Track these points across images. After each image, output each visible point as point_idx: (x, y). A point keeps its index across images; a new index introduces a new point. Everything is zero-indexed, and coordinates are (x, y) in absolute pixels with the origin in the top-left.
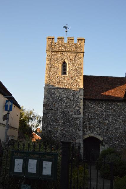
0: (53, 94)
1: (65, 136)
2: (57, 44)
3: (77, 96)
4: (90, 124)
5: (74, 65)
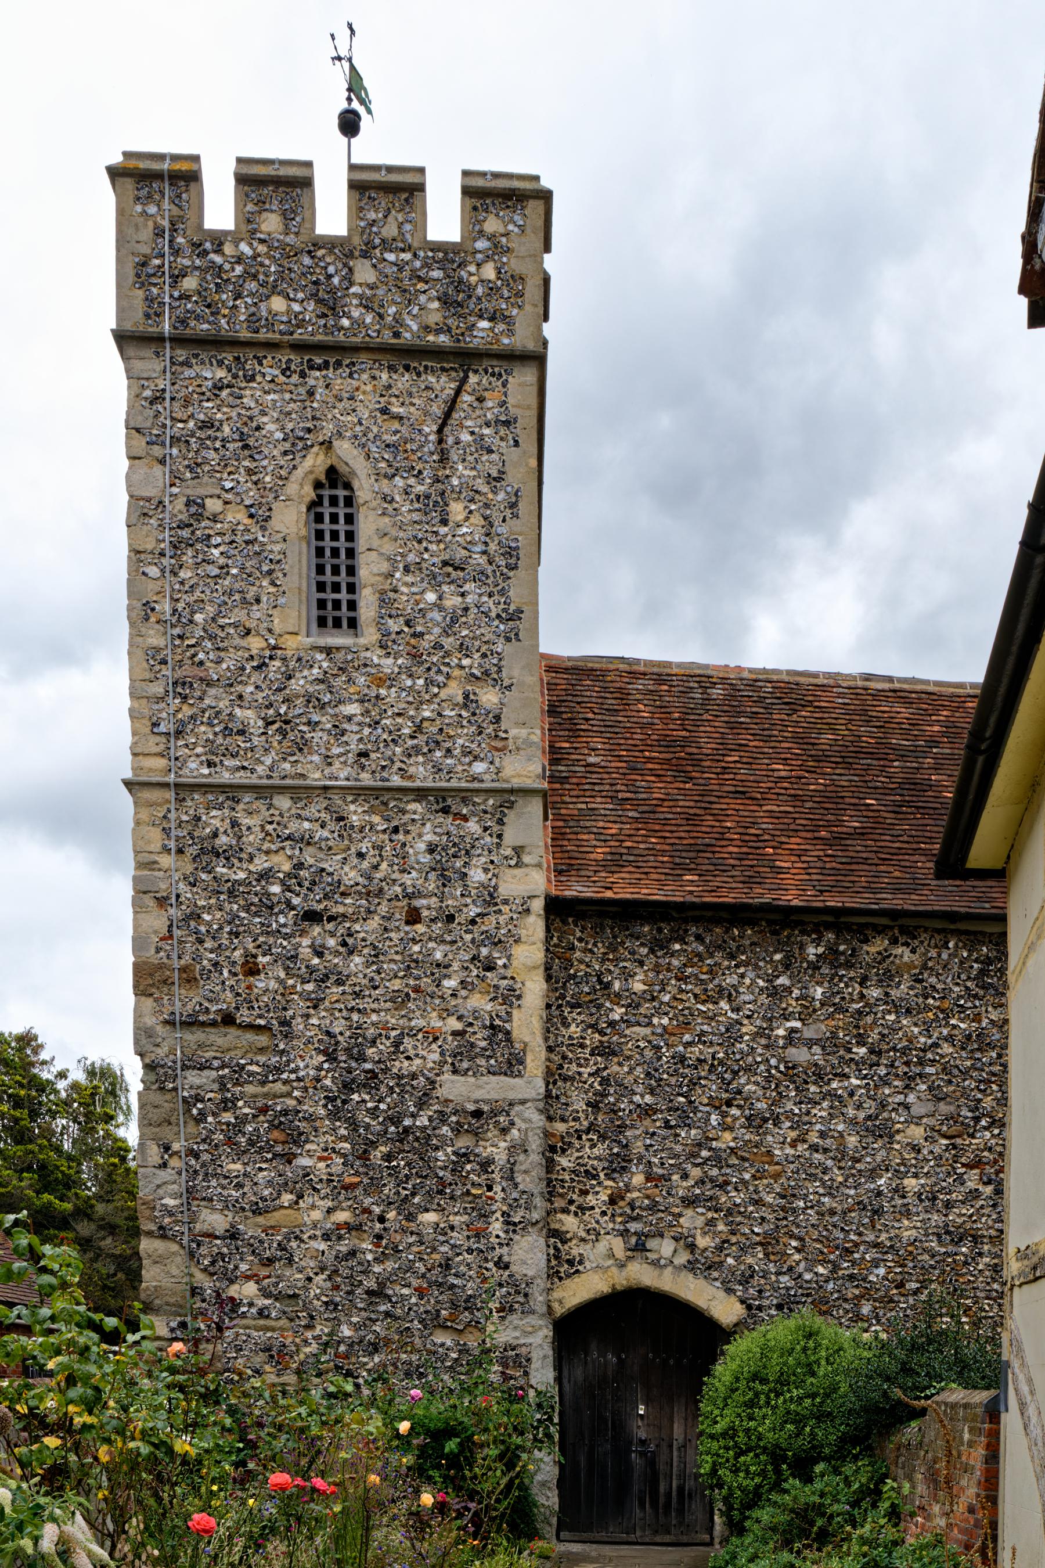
0: (227, 856)
1: (370, 1293)
4: (619, 1165)
5: (434, 506)
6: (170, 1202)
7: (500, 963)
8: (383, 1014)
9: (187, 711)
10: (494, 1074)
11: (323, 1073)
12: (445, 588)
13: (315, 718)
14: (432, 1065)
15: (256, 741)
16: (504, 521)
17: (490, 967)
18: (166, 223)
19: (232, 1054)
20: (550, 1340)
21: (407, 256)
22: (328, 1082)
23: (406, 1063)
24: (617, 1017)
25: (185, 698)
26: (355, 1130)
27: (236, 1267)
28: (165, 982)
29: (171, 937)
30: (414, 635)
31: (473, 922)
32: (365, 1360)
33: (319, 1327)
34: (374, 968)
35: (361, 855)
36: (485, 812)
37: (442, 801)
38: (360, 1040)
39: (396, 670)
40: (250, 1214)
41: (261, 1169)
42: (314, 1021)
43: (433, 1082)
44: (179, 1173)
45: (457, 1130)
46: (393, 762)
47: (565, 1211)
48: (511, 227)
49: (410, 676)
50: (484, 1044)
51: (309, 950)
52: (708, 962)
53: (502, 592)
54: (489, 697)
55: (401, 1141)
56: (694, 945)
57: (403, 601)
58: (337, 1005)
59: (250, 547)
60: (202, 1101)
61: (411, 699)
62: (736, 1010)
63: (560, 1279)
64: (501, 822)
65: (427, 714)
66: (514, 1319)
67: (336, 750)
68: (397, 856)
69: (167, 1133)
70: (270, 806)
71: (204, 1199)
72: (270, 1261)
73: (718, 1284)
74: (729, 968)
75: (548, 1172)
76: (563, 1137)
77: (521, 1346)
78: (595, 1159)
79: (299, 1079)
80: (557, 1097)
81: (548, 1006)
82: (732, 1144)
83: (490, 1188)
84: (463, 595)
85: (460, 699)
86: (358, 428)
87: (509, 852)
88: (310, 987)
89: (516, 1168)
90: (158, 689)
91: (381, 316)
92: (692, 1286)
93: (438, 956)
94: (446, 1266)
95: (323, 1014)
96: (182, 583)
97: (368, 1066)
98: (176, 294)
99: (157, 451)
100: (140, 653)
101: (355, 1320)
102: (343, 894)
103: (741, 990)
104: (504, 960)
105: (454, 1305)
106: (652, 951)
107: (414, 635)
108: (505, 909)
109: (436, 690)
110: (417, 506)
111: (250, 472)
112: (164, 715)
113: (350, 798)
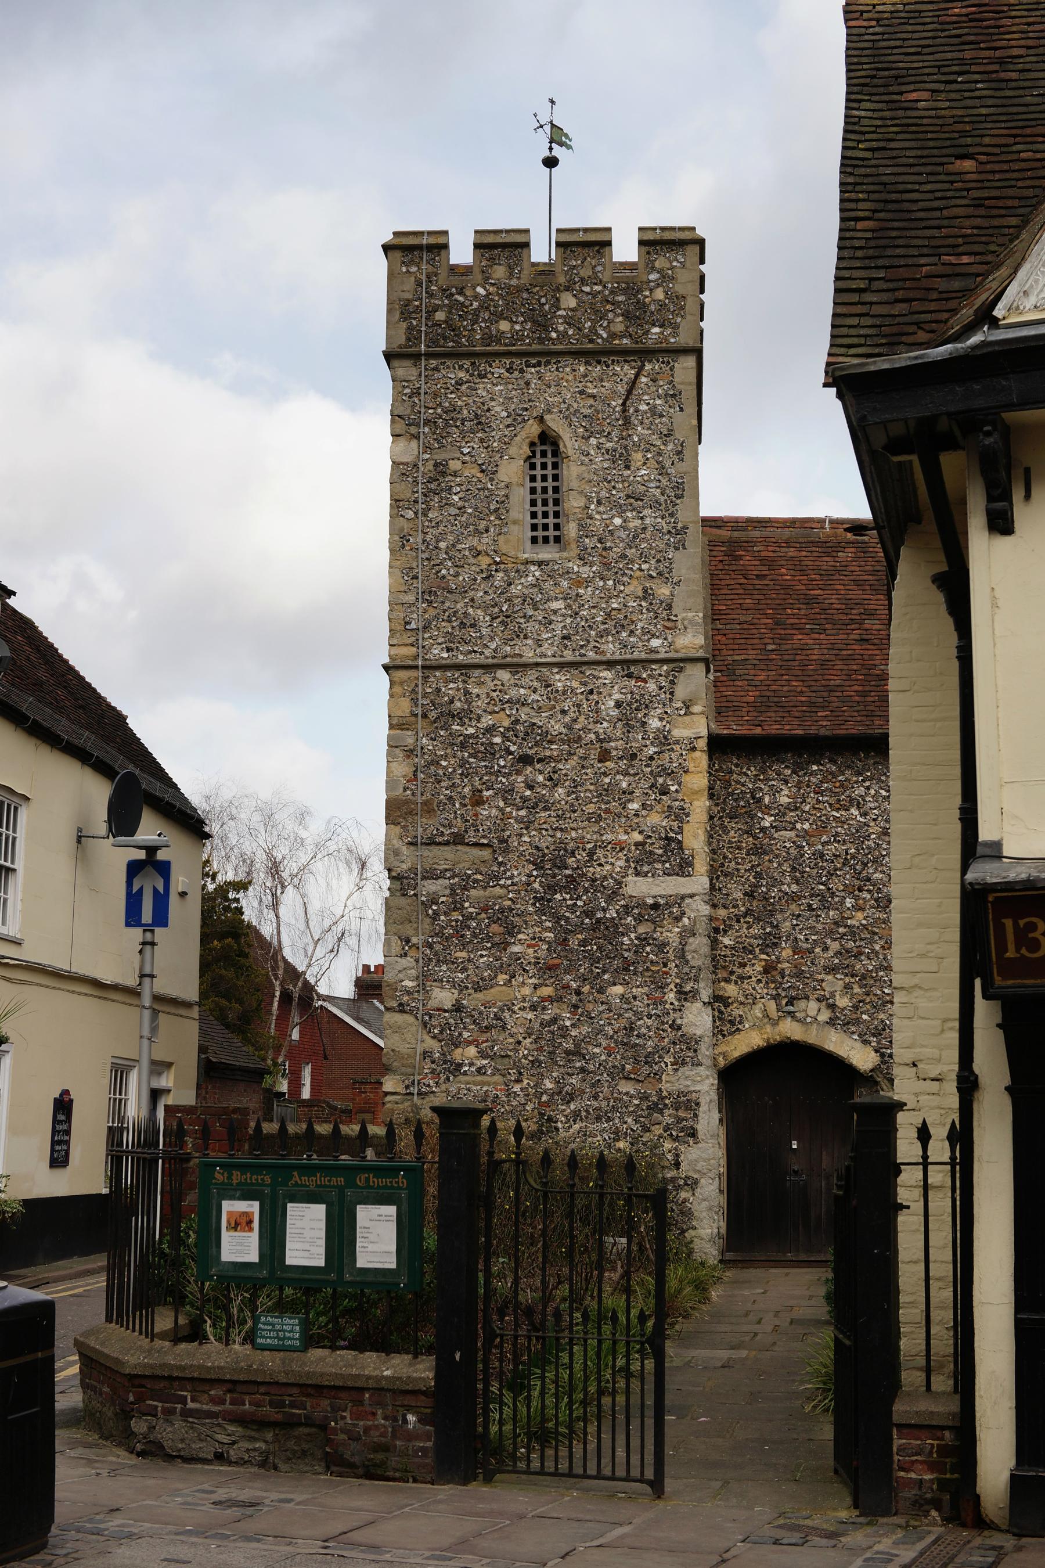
0: (460, 717)
1: (568, 1052)
2: (468, 293)
3: (654, 723)
4: (770, 942)
6: (409, 984)
7: (673, 788)
8: (580, 831)
9: (432, 612)
10: (669, 875)
11: (533, 878)
12: (629, 514)
13: (530, 612)
14: (619, 869)
15: (484, 631)
16: (673, 464)
17: (664, 792)
18: (424, 278)
19: (461, 866)
20: (715, 1087)
21: (598, 288)
22: (536, 885)
23: (599, 869)
24: (768, 824)
25: (430, 602)
26: (558, 922)
27: (460, 1034)
28: (410, 813)
29: (416, 779)
30: (605, 549)
31: (651, 758)
32: (564, 1107)
33: (526, 1082)
34: (574, 796)
35: (564, 712)
36: (660, 675)
37: (626, 667)
38: (562, 852)
39: (592, 575)
40: (471, 991)
41: (482, 956)
42: (526, 839)
43: (620, 883)
44: (417, 961)
45: (639, 919)
46: (588, 642)
47: (727, 981)
48: (675, 264)
49: (602, 579)
50: (660, 852)
51: (523, 785)
52: (840, 778)
53: (672, 515)
54: (664, 591)
55: (594, 930)
56: (828, 766)
57: (597, 525)
58: (544, 826)
59: (481, 493)
60: (437, 904)
61: (603, 595)
62: (864, 814)
63: (724, 1036)
64: (672, 682)
65: (615, 606)
66: (686, 1070)
67: (545, 636)
68: (591, 711)
69: (408, 930)
70: (494, 678)
71: (435, 981)
72: (488, 1028)
73: (856, 1037)
74: (857, 782)
75: (712, 950)
76: (724, 921)
77: (691, 1092)
78: (751, 937)
79: (513, 884)
80: (720, 889)
81: (711, 818)
82: (864, 922)
83: (665, 965)
84: (642, 518)
85: (640, 594)
86: (562, 406)
87: (679, 704)
88: (523, 813)
89: (687, 948)
90: (410, 598)
91: (580, 329)
92: (834, 1039)
93: (624, 785)
94: (630, 1028)
95: (533, 833)
96: (430, 521)
97: (568, 872)
98: (430, 323)
99: (413, 430)
100: (397, 572)
101: (554, 1074)
102: (551, 742)
103: (868, 799)
104: (676, 787)
105: (637, 1061)
106: (794, 772)
107: (605, 549)
108: (677, 747)
109: (622, 588)
110: (607, 457)
111: (482, 440)
112: (415, 616)
113: (556, 670)
